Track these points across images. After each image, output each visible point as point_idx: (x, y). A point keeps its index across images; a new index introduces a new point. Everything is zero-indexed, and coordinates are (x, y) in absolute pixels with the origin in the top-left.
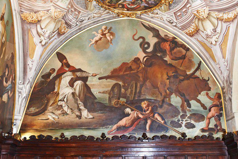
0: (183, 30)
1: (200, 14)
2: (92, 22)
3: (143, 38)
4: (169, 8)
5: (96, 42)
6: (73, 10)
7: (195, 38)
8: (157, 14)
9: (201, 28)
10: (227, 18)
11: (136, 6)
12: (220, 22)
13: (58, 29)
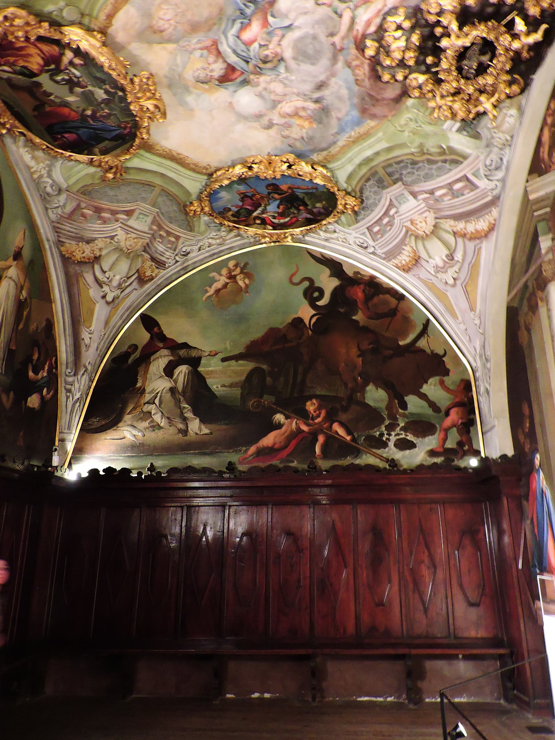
0: (390, 260)
1: (418, 227)
2: (207, 254)
3: (311, 280)
4: (356, 219)
5: (218, 291)
6: (162, 233)
7: (414, 274)
8: (335, 232)
9: (423, 254)
10: (474, 231)
11: (290, 220)
12: (460, 240)
13: (138, 271)
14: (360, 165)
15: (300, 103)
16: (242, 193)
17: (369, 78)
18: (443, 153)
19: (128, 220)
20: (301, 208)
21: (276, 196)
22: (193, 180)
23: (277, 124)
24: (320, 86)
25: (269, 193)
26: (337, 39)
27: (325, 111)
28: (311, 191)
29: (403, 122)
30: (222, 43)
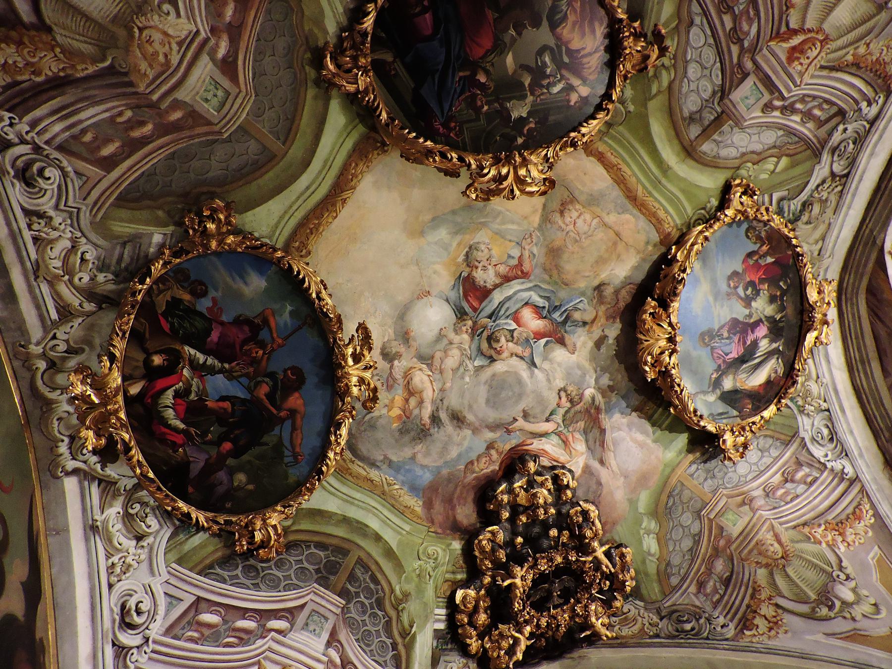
4: (211, 566)
6: (148, 128)
11: (176, 430)
14: (345, 520)
15: (428, 395)
16: (266, 322)
17: (476, 478)
18: (404, 634)
19: (213, 59)
20: (227, 446)
21: (263, 390)
22: (279, 222)
23: (391, 367)
24: (458, 419)
25: (272, 375)
26: (521, 423)
27: (422, 434)
28: (287, 453)
29: (430, 550)
30: (523, 283)
